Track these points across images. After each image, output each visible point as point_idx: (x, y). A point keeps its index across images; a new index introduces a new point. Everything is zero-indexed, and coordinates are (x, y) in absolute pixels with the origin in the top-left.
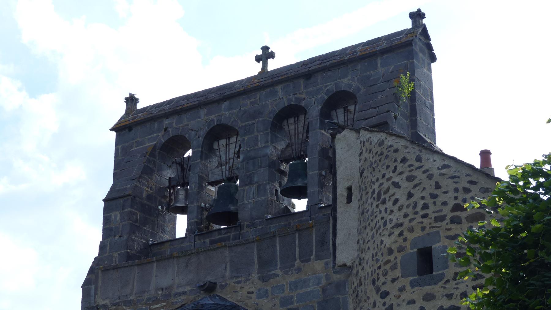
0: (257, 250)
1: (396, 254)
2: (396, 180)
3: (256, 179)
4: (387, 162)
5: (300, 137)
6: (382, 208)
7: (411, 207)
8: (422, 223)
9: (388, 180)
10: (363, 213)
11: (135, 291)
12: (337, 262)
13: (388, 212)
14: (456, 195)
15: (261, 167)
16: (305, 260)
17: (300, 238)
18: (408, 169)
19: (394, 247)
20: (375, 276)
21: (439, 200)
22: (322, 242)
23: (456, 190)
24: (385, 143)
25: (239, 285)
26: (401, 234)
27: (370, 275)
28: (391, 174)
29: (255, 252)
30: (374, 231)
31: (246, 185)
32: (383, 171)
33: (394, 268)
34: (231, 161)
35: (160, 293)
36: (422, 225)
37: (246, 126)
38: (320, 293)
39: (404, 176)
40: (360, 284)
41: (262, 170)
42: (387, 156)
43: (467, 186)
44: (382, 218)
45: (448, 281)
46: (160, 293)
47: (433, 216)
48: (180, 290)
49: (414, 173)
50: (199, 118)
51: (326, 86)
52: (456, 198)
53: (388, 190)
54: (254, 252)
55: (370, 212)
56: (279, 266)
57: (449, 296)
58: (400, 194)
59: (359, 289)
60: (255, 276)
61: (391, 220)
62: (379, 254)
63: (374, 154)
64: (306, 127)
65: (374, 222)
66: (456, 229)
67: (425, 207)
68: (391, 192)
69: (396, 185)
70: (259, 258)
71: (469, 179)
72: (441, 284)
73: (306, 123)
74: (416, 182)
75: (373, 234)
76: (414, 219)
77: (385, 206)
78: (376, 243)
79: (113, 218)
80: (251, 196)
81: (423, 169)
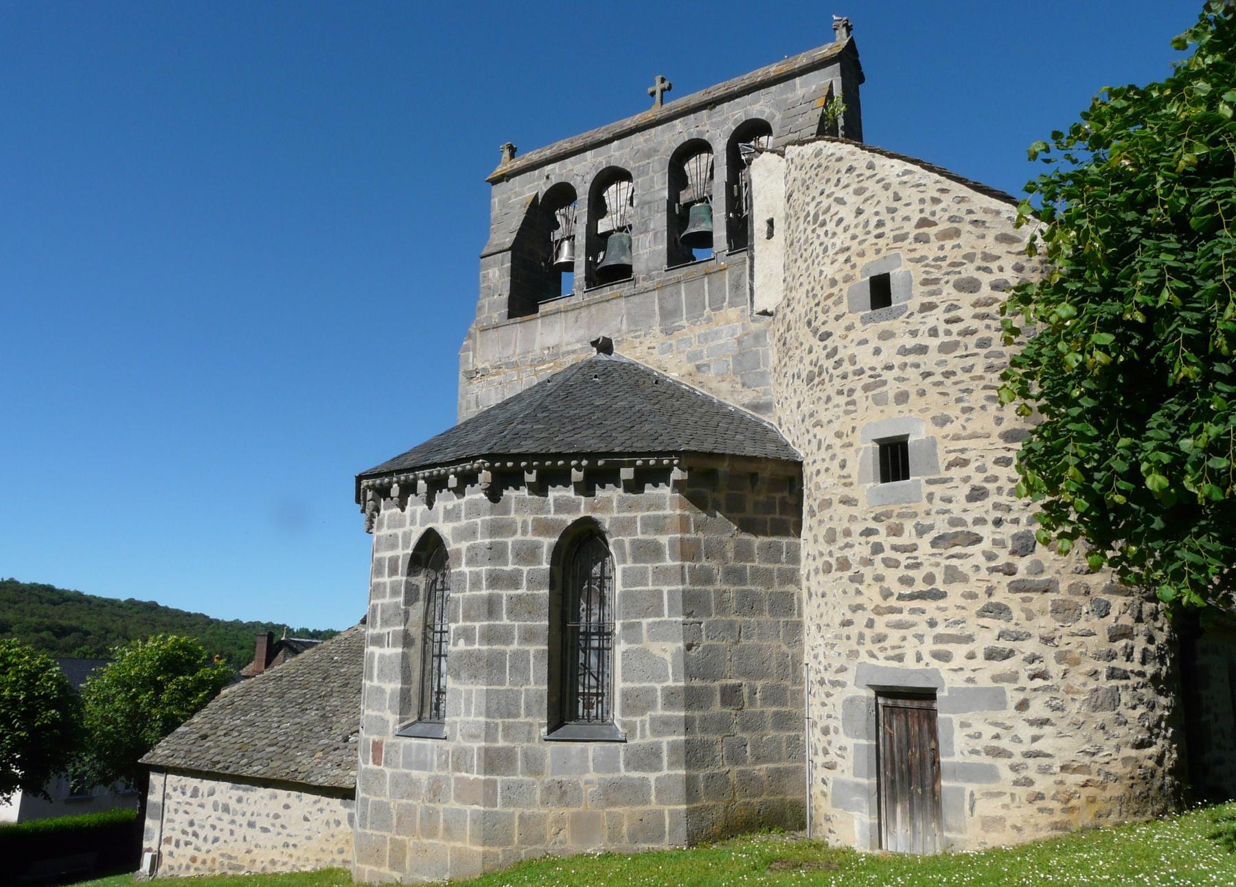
1: (841, 285)
2: (841, 196)
3: (652, 226)
4: (826, 174)
5: (703, 177)
6: (821, 231)
7: (861, 226)
8: (876, 244)
9: (828, 196)
10: (792, 244)
11: (518, 351)
12: (755, 309)
13: (830, 235)
14: (922, 206)
15: (658, 212)
16: (717, 307)
17: (709, 283)
18: (857, 180)
19: (838, 277)
20: (813, 317)
21: (899, 216)
22: (737, 287)
23: (922, 201)
24: (824, 152)
25: (638, 340)
26: (847, 261)
27: (803, 315)
28: (833, 189)
29: (657, 302)
30: (810, 261)
31: (641, 233)
32: (820, 188)
33: (838, 302)
34: (623, 209)
35: (546, 352)
36: (876, 247)
37: (640, 166)
38: (736, 345)
39: (851, 189)
40: (789, 329)
42: (827, 168)
43: (937, 195)
44: (821, 244)
45: (912, 314)
46: (546, 352)
47: (892, 234)
48: (570, 348)
49: (864, 184)
51: (733, 116)
52: (922, 211)
53: (828, 209)
55: (802, 241)
56: (684, 317)
57: (914, 333)
58: (846, 213)
59: (788, 335)
60: (657, 329)
61: (834, 245)
62: (818, 288)
63: (808, 169)
64: (709, 165)
65: (809, 251)
66: (922, 250)
67: (880, 224)
68: (833, 211)
69: (840, 201)
70: (661, 308)
71: (939, 186)
72: (902, 318)
73: (710, 160)
74: (867, 194)
75: (808, 266)
76: (864, 241)
77: (825, 229)
78: (812, 276)
79: (491, 275)
80: (647, 245)
81: (877, 178)
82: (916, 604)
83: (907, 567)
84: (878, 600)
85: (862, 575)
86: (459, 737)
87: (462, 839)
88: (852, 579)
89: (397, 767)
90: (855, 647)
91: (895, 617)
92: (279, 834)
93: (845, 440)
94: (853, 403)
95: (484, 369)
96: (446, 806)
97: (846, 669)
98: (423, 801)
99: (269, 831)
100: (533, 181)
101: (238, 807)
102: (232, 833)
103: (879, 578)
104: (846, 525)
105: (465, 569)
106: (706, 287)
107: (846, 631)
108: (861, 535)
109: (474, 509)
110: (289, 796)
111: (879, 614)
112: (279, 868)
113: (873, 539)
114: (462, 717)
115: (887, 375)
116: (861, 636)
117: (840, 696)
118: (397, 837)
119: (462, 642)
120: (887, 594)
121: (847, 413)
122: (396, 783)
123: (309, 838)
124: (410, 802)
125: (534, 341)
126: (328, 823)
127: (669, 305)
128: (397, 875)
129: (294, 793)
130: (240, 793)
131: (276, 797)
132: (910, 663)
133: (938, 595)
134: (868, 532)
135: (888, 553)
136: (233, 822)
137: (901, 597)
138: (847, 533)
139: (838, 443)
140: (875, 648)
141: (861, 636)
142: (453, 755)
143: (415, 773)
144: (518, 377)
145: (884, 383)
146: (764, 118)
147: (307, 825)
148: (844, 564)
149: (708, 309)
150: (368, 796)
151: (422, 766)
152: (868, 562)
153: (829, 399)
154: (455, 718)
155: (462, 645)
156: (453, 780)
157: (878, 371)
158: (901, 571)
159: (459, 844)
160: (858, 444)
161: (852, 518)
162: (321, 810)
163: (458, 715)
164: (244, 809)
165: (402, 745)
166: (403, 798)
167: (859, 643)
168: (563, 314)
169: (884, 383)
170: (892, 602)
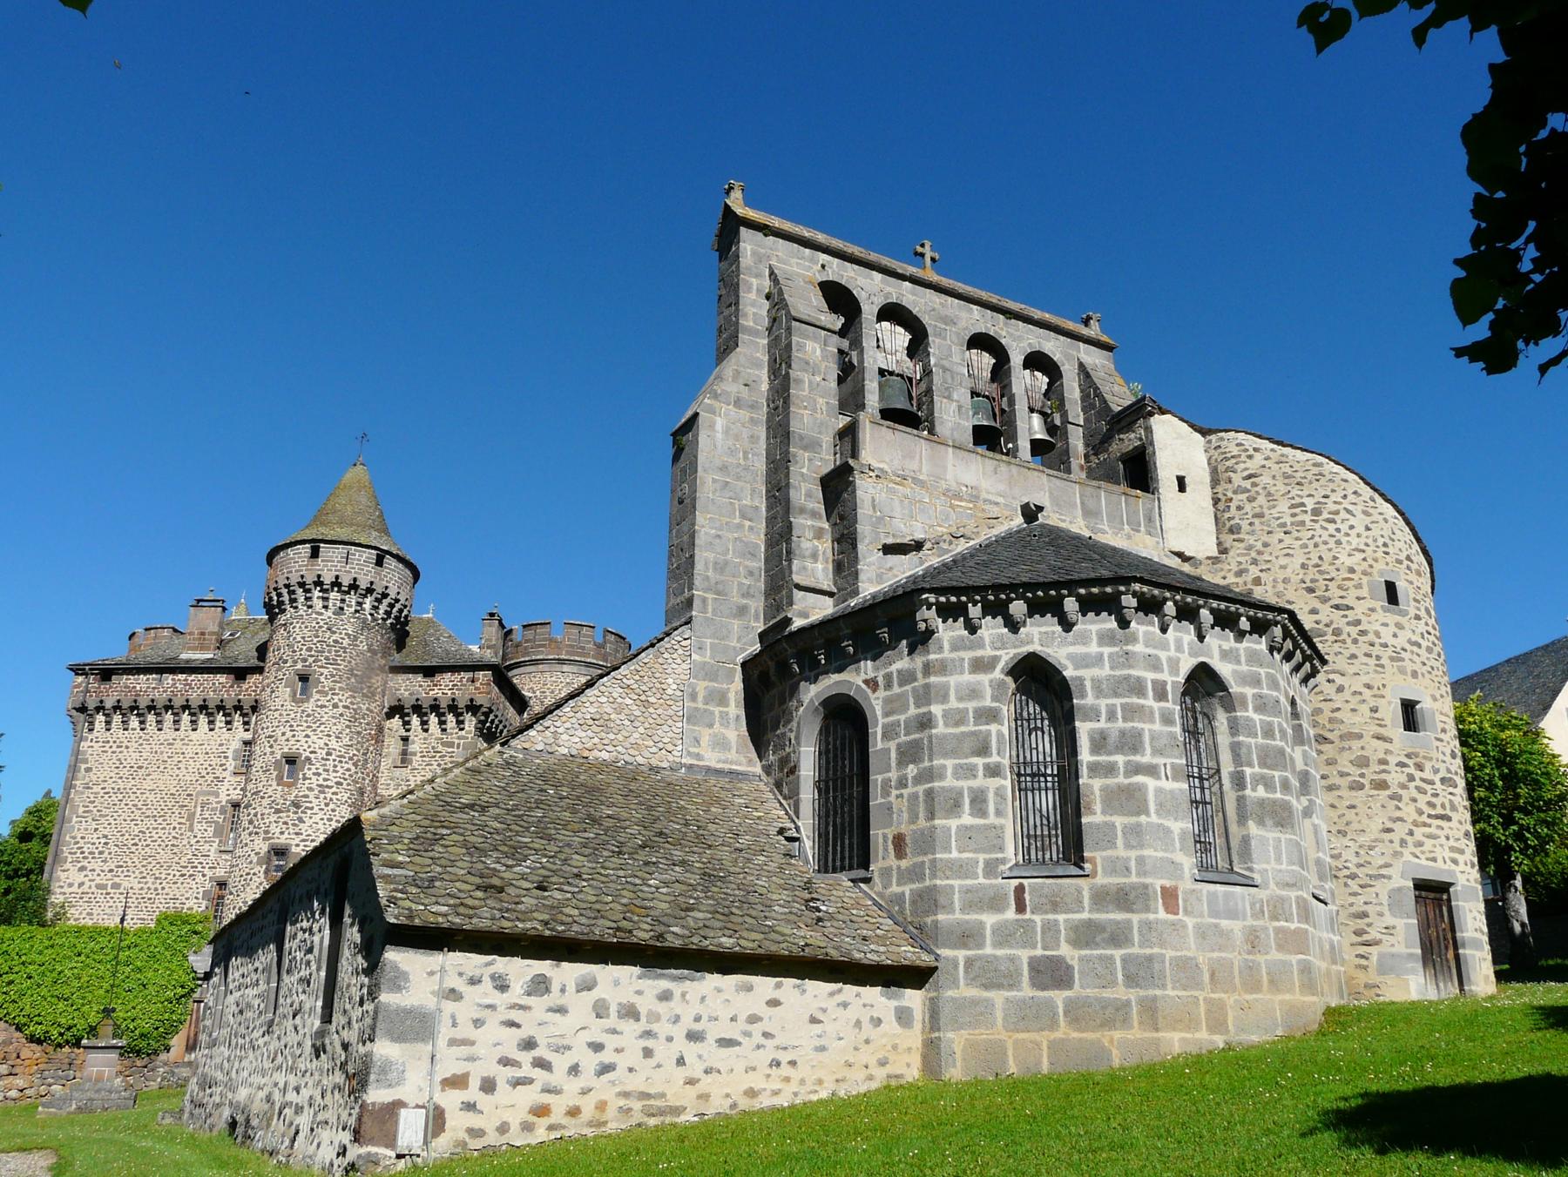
3: (955, 397)
11: (924, 470)
29: (1078, 495)
35: (964, 489)
41: (963, 390)
48: (990, 497)
50: (872, 280)
70: (1082, 503)
82: (1439, 822)
83: (1433, 795)
84: (1415, 816)
85: (1401, 796)
86: (1272, 885)
87: (1291, 990)
88: (1392, 798)
89: (1201, 916)
90: (1399, 849)
91: (1427, 830)
92: (758, 1047)
93: (1375, 691)
94: (1383, 666)
95: (882, 470)
96: (1268, 957)
97: (1391, 865)
98: (1240, 954)
99: (739, 1044)
100: (802, 258)
101: (662, 1008)
102: (648, 1053)
103: (1415, 800)
104: (1382, 756)
105: (1251, 713)
106: (1123, 505)
107: (1387, 836)
108: (1397, 765)
109: (1253, 657)
110: (778, 986)
111: (1416, 826)
112: (765, 1101)
113: (1406, 770)
114: (1273, 865)
115: (1404, 655)
116: (1403, 842)
117: (1382, 888)
118: (1213, 995)
119: (1261, 789)
120: (1421, 813)
121: (1376, 671)
122: (1202, 933)
123: (822, 1049)
124: (1223, 955)
125: (945, 468)
126: (858, 1024)
127: (1091, 504)
128: (1219, 1040)
129: (789, 982)
130: (664, 984)
131: (750, 988)
132: (1440, 864)
133: (1449, 819)
134: (1402, 765)
135: (1418, 783)
136: (648, 1034)
137: (1429, 816)
138: (1383, 762)
139: (1367, 693)
140: (1417, 851)
141: (1403, 842)
142: (1268, 906)
143: (1225, 923)
144: (930, 500)
145: (1403, 660)
146: (1055, 359)
147: (817, 1028)
148: (1382, 785)
149: (1126, 527)
150: (1164, 951)
151: (1233, 914)
152: (1404, 787)
153: (1353, 656)
154: (1265, 866)
155: (1261, 792)
156: (1271, 929)
157: (1398, 650)
158: (1428, 798)
159: (1288, 997)
160: (1388, 697)
161: (1387, 752)
162: (845, 1005)
163: (1268, 863)
164: (678, 1011)
165: (1205, 892)
166: (1213, 951)
167: (1401, 846)
168: (979, 457)
169: (1403, 660)
170: (1424, 818)
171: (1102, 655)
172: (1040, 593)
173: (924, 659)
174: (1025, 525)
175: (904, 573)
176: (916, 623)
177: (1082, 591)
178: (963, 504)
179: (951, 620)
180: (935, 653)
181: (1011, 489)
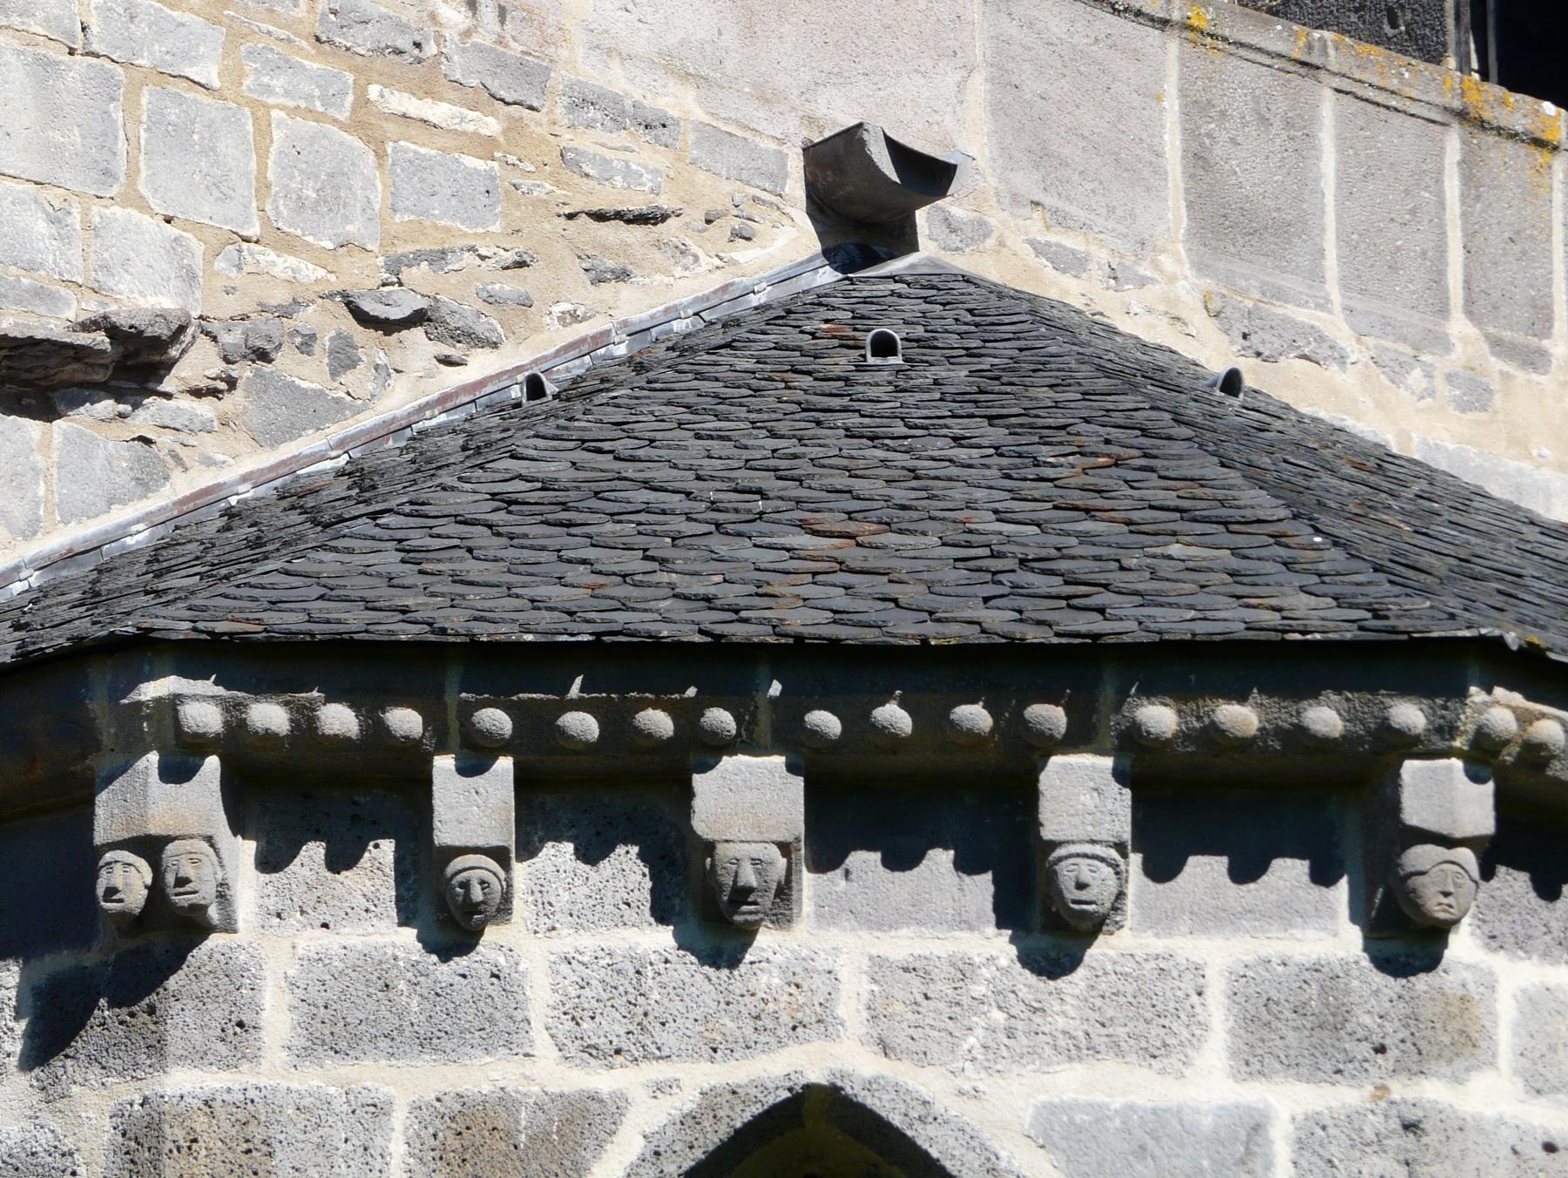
0: (1183, 93)
29: (1172, 105)
48: (617, 80)
54: (1159, 98)
70: (1198, 160)
106: (1452, 185)
144: (234, 74)
149: (1459, 326)
171: (1256, 1128)
172: (894, 715)
173: (127, 1092)
174: (827, 276)
175: (30, 531)
176: (89, 859)
177: (1160, 717)
178: (438, 112)
179: (314, 852)
180: (198, 1057)
181: (750, 32)
